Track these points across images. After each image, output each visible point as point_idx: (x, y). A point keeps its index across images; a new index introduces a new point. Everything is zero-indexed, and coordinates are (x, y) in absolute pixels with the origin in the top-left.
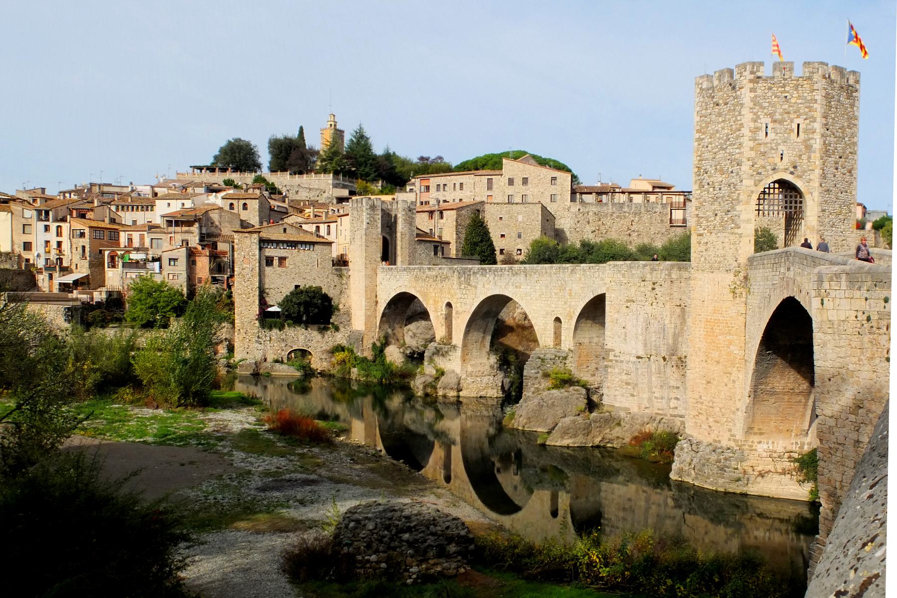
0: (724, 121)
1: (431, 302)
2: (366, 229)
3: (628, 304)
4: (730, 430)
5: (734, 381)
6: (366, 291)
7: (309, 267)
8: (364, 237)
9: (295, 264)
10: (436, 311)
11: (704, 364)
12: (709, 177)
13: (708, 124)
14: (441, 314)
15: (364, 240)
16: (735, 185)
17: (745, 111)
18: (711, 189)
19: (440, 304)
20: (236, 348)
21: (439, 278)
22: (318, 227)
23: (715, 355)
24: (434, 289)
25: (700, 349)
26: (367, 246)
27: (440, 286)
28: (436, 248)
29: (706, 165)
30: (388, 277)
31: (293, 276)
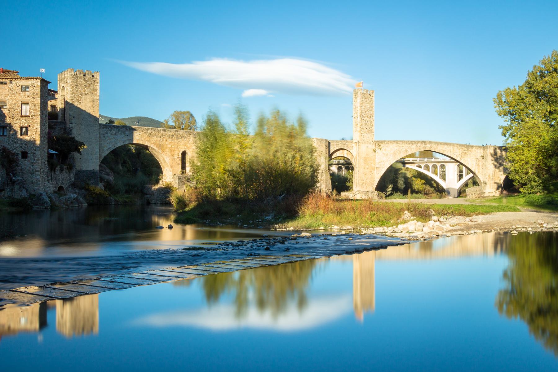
0: (368, 104)
3: (321, 153)
4: (372, 187)
5: (373, 173)
11: (364, 169)
12: (364, 118)
13: (363, 103)
14: (178, 158)
16: (372, 122)
17: (374, 103)
18: (365, 121)
19: (177, 152)
21: (175, 136)
23: (367, 167)
25: (362, 165)
27: (176, 141)
29: (363, 114)
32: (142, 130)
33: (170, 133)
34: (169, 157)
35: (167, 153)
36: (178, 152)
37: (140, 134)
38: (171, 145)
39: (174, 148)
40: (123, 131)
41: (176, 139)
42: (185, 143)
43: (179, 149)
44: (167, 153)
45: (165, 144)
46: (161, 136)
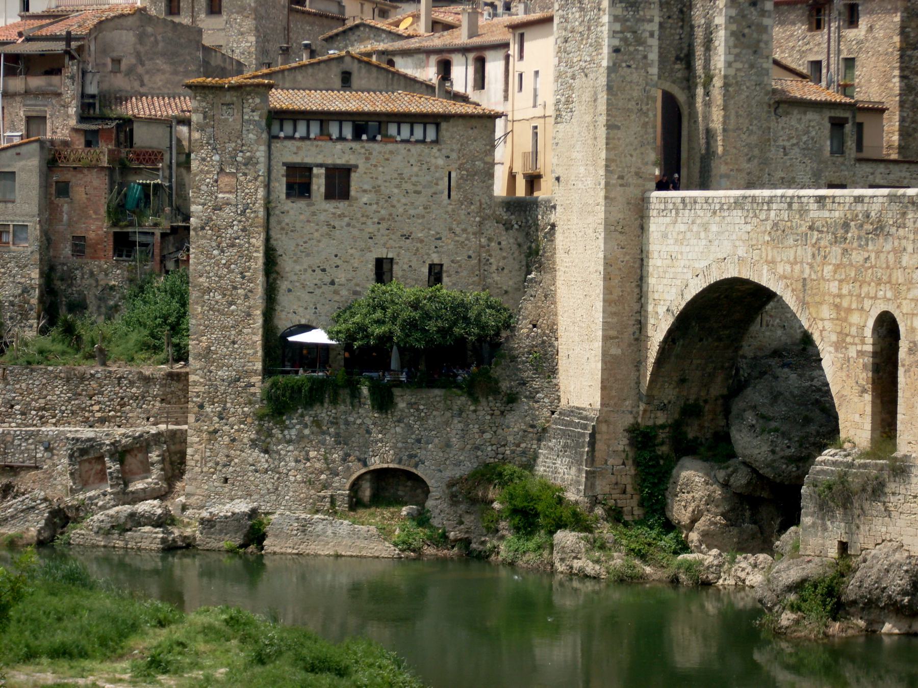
1: (826, 312)
2: (612, 69)
6: (607, 278)
7: (422, 200)
8: (603, 97)
9: (376, 189)
10: (840, 345)
14: (861, 353)
15: (602, 107)
19: (855, 318)
20: (190, 462)
22: (445, 68)
24: (837, 267)
26: (610, 126)
27: (857, 257)
28: (837, 125)
30: (683, 228)
31: (371, 228)
32: (755, 205)
33: (837, 214)
34: (832, 349)
35: (824, 329)
36: (862, 324)
37: (749, 228)
38: (841, 281)
39: (848, 298)
40: (705, 220)
41: (855, 244)
42: (888, 267)
43: (867, 304)
44: (824, 329)
45: (819, 274)
46: (809, 232)
